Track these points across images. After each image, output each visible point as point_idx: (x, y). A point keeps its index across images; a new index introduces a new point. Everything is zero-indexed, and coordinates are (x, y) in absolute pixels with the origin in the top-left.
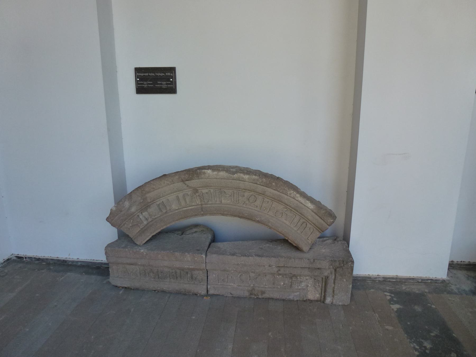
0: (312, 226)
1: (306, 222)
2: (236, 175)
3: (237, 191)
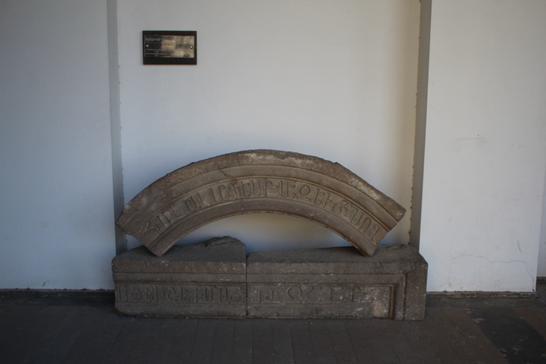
0: (377, 223)
2: (286, 159)
3: (287, 180)
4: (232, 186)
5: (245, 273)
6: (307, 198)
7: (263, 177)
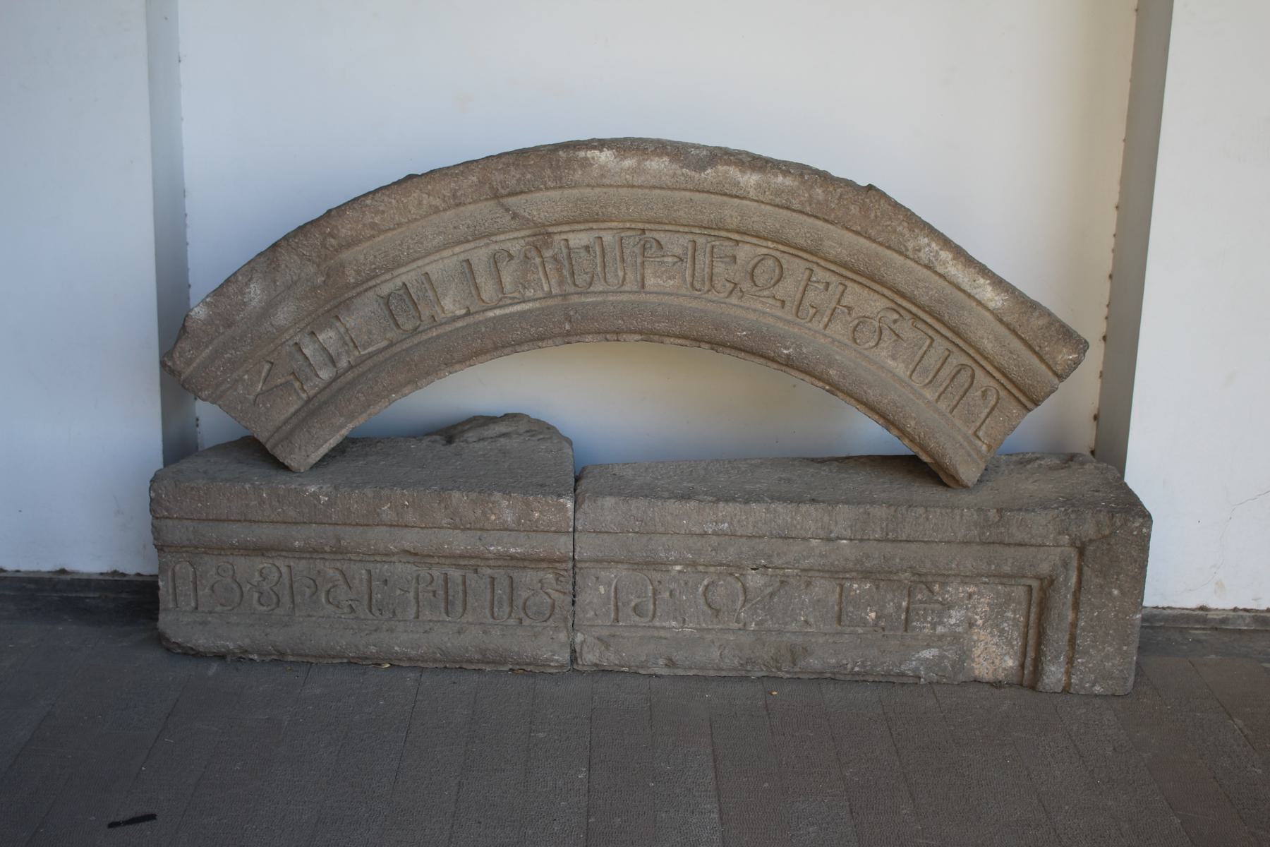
0: (993, 383)
1: (972, 368)
2: (709, 171)
3: (709, 239)
4: (534, 253)
5: (571, 529)
6: (774, 297)
7: (633, 226)
